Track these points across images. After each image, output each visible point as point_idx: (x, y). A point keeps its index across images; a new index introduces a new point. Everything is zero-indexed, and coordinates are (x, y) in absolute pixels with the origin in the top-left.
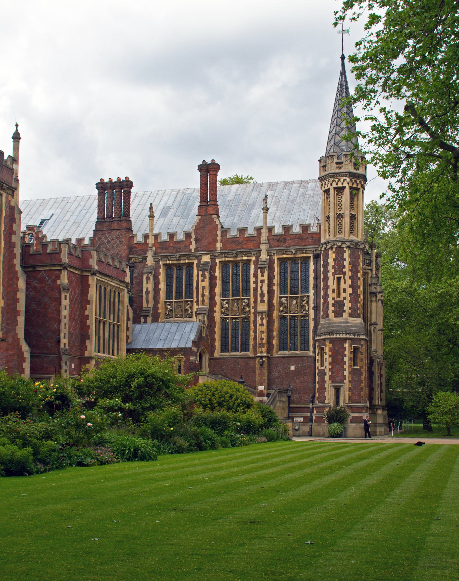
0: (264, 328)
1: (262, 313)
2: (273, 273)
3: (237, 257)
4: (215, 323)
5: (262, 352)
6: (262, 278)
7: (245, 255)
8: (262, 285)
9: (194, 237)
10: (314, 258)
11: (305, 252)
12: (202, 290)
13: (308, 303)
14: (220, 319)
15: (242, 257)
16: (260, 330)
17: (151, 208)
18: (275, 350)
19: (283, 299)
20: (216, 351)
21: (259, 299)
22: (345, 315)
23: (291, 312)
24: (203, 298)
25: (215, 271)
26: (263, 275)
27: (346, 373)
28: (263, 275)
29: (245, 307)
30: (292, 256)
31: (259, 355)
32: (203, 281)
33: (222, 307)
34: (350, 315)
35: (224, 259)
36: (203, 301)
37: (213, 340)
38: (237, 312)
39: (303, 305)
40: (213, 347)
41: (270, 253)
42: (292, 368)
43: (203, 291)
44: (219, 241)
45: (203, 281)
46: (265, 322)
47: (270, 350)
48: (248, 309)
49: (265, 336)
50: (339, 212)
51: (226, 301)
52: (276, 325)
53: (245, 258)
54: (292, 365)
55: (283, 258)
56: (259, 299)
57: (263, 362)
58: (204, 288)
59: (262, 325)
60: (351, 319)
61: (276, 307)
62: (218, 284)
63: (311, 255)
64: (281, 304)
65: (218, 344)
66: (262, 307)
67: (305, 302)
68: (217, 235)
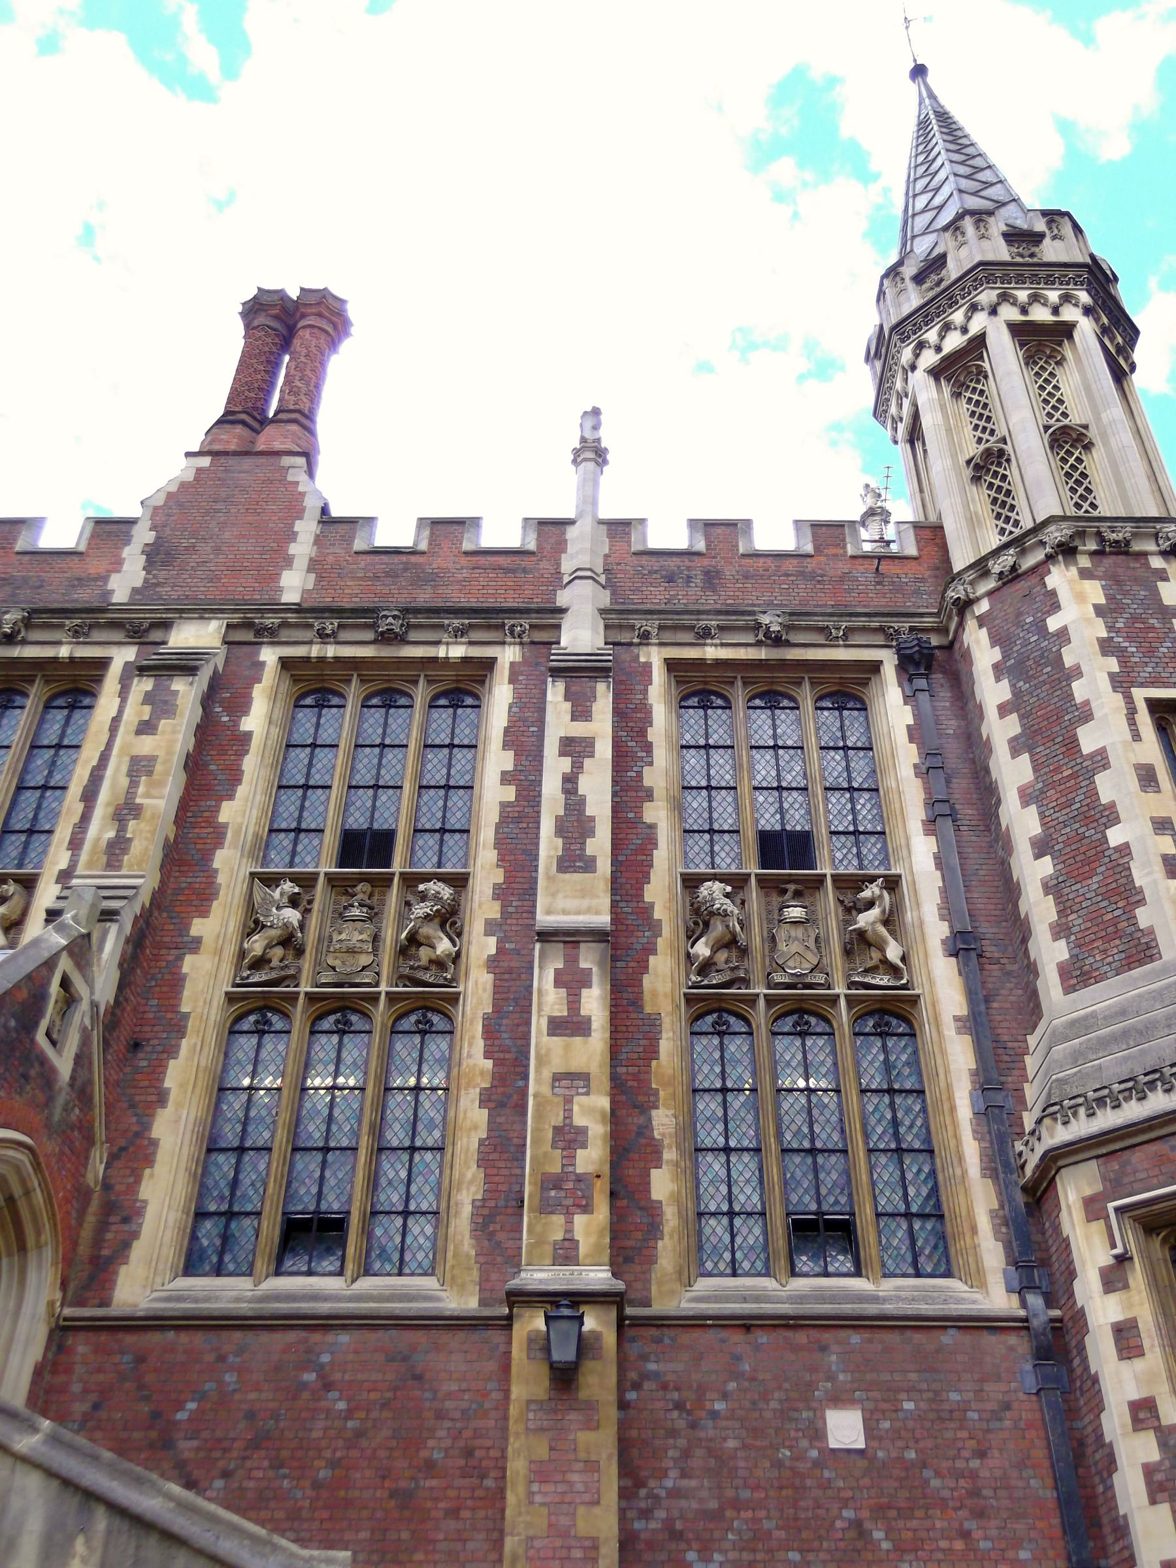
0: (591, 1052)
1: (570, 938)
2: (643, 733)
3: (402, 640)
4: (178, 1027)
5: (566, 1253)
6: (579, 729)
7: (460, 632)
8: (577, 767)
10: (901, 668)
11: (845, 637)
12: (124, 782)
14: (219, 999)
15: (437, 643)
16: (557, 1064)
20: (138, 1250)
21: (549, 845)
23: (778, 978)
24: (122, 829)
25: (241, 705)
26: (581, 713)
28: (581, 713)
29: (428, 930)
30: (762, 654)
31: (540, 1276)
33: (253, 925)
35: (315, 651)
36: (117, 848)
37: (135, 1152)
38: (365, 960)
39: (861, 934)
40: (119, 1214)
42: (845, 1428)
43: (134, 784)
44: (301, 563)
45: (146, 728)
46: (594, 1002)
47: (629, 1243)
48: (444, 946)
49: (591, 1110)
51: (288, 887)
53: (457, 651)
54: (838, 1400)
55: (700, 664)
56: (549, 845)
57: (585, 1346)
58: (140, 767)
59: (570, 1025)
61: (666, 930)
62: (246, 778)
63: (889, 660)
64: (699, 920)
67: (875, 913)
68: (292, 536)
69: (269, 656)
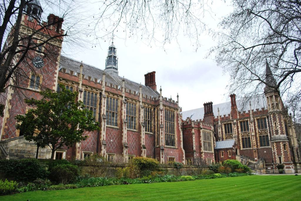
0: (255, 140)
1: (253, 136)
4: (240, 140)
6: (252, 125)
9: (231, 115)
13: (267, 131)
17: (218, 109)
18: (259, 146)
19: (259, 131)
21: (252, 131)
22: (279, 134)
25: (238, 124)
26: (252, 124)
27: (282, 152)
28: (252, 124)
31: (254, 148)
32: (235, 128)
33: (241, 135)
34: (281, 134)
36: (235, 133)
37: (240, 145)
41: (254, 118)
42: (265, 152)
45: (235, 128)
46: (254, 138)
47: (257, 146)
49: (255, 142)
50: (272, 103)
52: (258, 139)
53: (246, 120)
56: (252, 131)
57: (255, 150)
58: (235, 130)
60: (281, 135)
63: (266, 117)
64: (259, 132)
65: (241, 146)
66: (253, 134)
69: (238, 121)
